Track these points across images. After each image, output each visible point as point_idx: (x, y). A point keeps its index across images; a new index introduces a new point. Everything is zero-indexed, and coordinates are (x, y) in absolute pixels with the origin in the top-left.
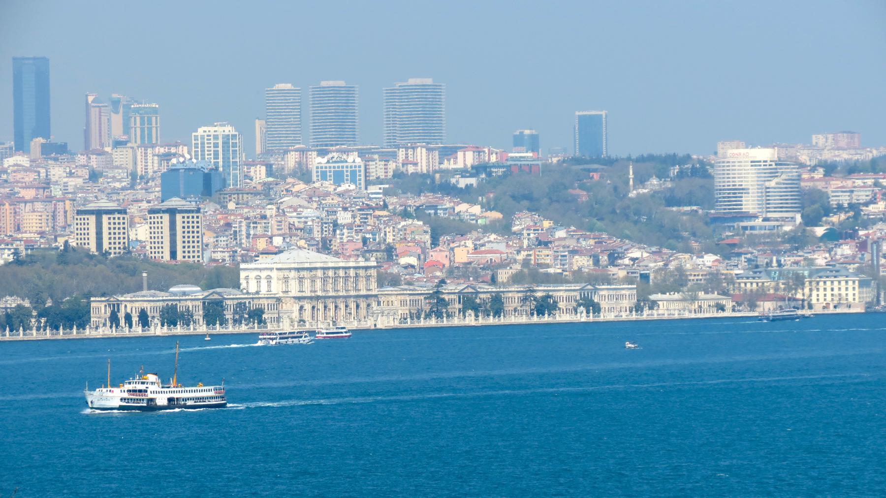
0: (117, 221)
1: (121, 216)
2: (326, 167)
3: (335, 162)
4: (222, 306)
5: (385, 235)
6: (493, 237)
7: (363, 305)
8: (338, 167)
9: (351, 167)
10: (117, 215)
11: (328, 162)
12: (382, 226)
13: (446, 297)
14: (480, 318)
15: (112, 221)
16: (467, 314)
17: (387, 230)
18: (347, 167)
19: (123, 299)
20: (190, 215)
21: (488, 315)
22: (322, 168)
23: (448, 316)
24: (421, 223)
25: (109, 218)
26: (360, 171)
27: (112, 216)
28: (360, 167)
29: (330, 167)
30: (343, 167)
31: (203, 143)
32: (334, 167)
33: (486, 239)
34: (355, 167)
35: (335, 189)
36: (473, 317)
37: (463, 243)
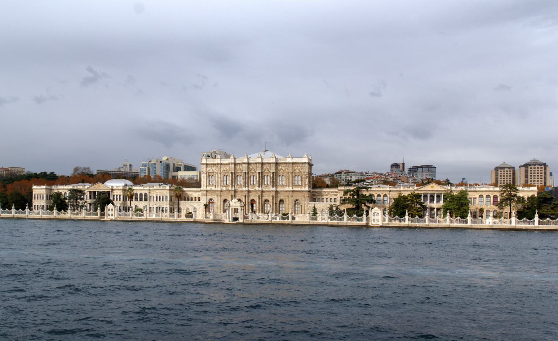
27: (502, 170)
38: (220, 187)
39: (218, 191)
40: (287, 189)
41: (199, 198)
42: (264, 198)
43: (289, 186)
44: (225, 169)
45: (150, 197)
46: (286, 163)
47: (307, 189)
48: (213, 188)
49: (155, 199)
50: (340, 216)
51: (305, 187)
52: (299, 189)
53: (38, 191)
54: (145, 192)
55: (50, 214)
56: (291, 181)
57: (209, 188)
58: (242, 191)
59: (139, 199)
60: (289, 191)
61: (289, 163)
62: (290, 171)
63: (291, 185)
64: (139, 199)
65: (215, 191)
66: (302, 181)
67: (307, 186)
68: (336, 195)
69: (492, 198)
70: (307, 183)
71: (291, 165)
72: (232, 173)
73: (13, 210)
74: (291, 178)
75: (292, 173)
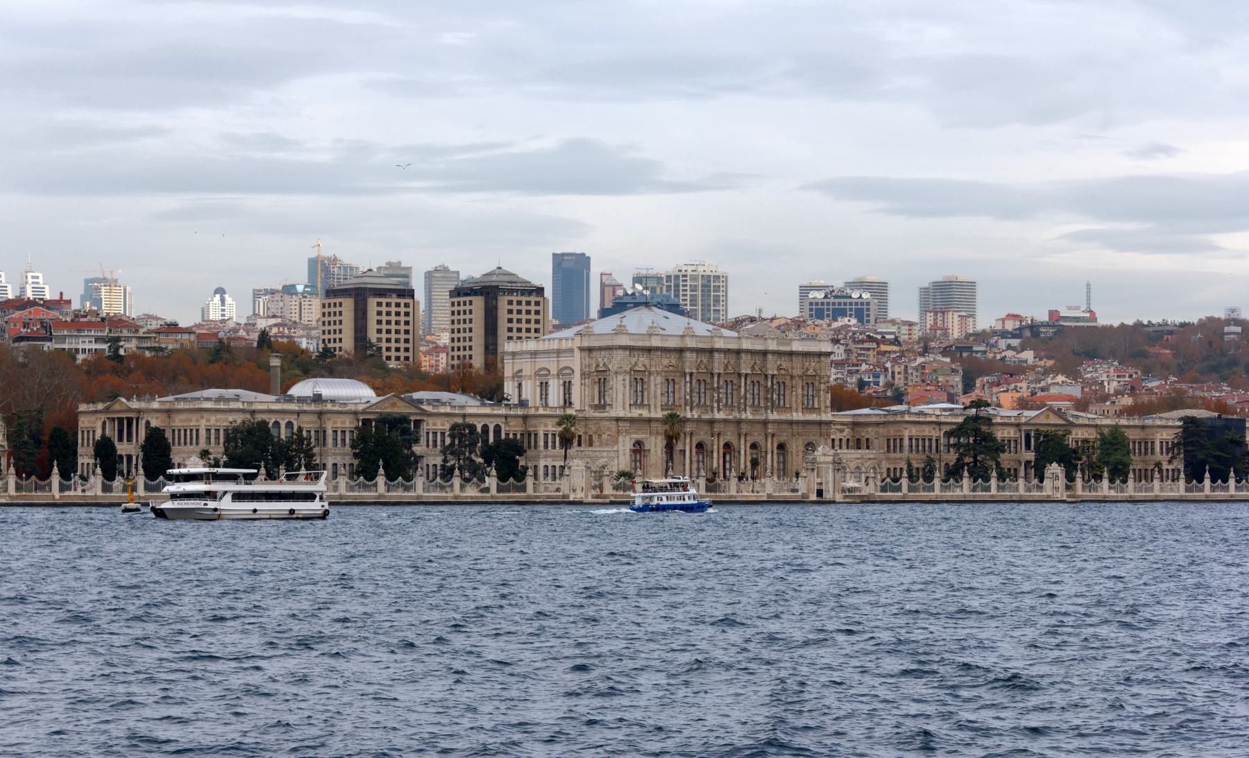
0: (393, 309)
1: (402, 301)
2: (823, 304)
3: (836, 297)
4: (405, 431)
5: (893, 377)
6: (1060, 378)
7: (796, 446)
8: (840, 304)
9: (857, 304)
10: (394, 300)
11: (826, 297)
12: (888, 365)
13: (1000, 434)
14: (1079, 483)
15: (384, 309)
16: (1048, 473)
17: (897, 369)
18: (851, 304)
19: (143, 405)
20: (524, 299)
21: (1098, 478)
22: (817, 304)
23: (1002, 477)
24: (948, 360)
25: (379, 304)
26: (868, 310)
27: (384, 301)
28: (868, 304)
29: (828, 304)
30: (845, 304)
31: (677, 286)
32: (834, 304)
33: (1049, 381)
34: (862, 304)
35: (829, 325)
36: (1061, 482)
37: (1012, 386)
38: (659, 410)
39: (657, 420)
42: (750, 440)
44: (666, 362)
46: (791, 354)
48: (645, 413)
49: (541, 443)
52: (813, 417)
53: (220, 416)
55: (366, 487)
57: (636, 413)
58: (712, 422)
59: (213, 431)
60: (798, 422)
64: (213, 431)
65: (649, 420)
66: (819, 397)
68: (842, 431)
70: (828, 403)
72: (691, 374)
73: (381, 480)
74: (800, 391)
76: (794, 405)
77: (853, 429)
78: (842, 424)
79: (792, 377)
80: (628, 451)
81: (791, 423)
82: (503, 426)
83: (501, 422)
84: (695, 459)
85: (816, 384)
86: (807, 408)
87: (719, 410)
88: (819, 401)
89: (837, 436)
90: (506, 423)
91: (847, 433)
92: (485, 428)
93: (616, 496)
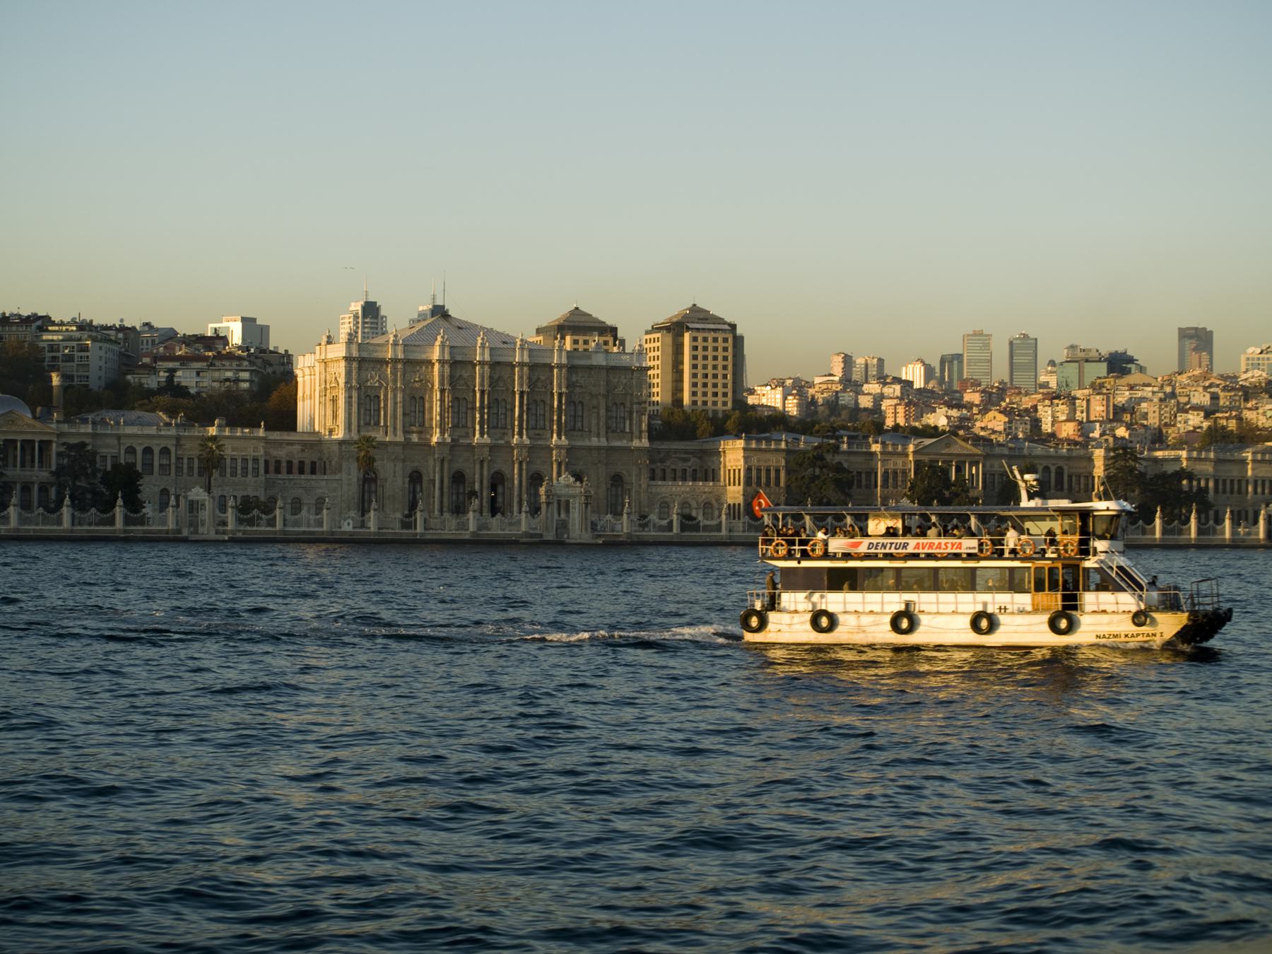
38: (399, 433)
40: (594, 441)
41: (290, 463)
43: (598, 436)
45: (179, 459)
46: (591, 368)
47: (645, 443)
50: (103, 512)
51: (640, 438)
52: (624, 443)
54: (164, 443)
56: (603, 419)
60: (599, 449)
61: (599, 368)
62: (602, 391)
63: (603, 431)
66: (631, 420)
67: (645, 435)
68: (686, 460)
69: (1053, 475)
70: (644, 426)
71: (604, 373)
74: (603, 412)
75: (606, 397)
76: (594, 429)
77: (700, 458)
78: (686, 452)
79: (592, 395)
80: (355, 480)
81: (590, 449)
82: (173, 449)
83: (171, 444)
84: (445, 490)
85: (628, 404)
86: (614, 431)
87: (482, 434)
88: (631, 425)
89: (680, 466)
90: (178, 445)
91: (693, 462)
92: (148, 451)
93: (244, 532)
